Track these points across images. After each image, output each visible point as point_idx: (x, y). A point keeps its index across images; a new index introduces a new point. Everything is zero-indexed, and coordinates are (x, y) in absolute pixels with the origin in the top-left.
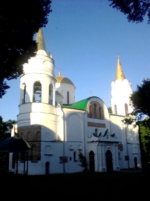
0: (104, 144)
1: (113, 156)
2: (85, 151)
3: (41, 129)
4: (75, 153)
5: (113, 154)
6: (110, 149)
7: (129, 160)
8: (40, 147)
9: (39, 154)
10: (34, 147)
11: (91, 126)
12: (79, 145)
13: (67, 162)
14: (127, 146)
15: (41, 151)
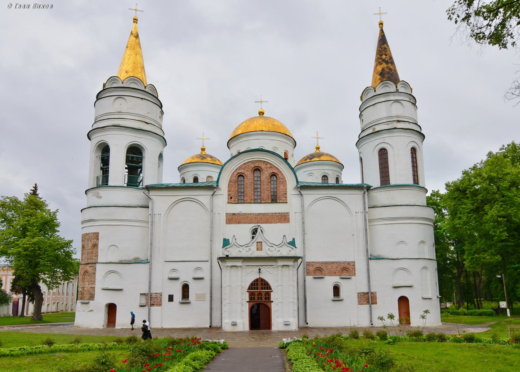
0: (239, 263)
1: (272, 293)
2: (211, 280)
3: (98, 239)
4: (186, 288)
5: (272, 287)
6: (263, 276)
7: (376, 303)
8: (94, 274)
9: (91, 288)
10: (86, 274)
11: (239, 223)
12: (198, 269)
13: (160, 305)
14: (368, 265)
15: (96, 283)
